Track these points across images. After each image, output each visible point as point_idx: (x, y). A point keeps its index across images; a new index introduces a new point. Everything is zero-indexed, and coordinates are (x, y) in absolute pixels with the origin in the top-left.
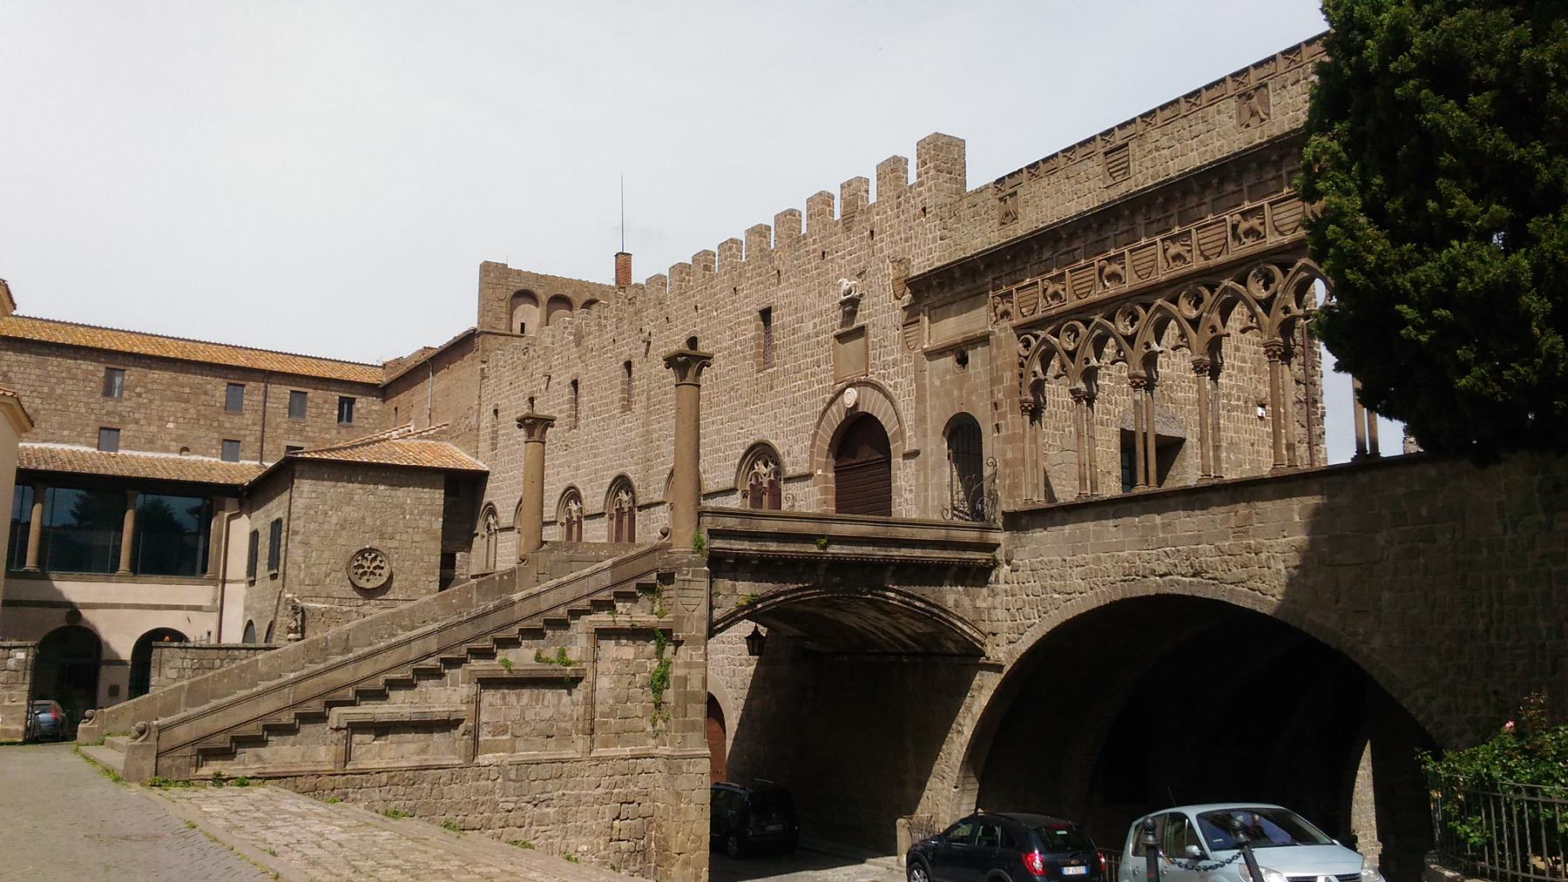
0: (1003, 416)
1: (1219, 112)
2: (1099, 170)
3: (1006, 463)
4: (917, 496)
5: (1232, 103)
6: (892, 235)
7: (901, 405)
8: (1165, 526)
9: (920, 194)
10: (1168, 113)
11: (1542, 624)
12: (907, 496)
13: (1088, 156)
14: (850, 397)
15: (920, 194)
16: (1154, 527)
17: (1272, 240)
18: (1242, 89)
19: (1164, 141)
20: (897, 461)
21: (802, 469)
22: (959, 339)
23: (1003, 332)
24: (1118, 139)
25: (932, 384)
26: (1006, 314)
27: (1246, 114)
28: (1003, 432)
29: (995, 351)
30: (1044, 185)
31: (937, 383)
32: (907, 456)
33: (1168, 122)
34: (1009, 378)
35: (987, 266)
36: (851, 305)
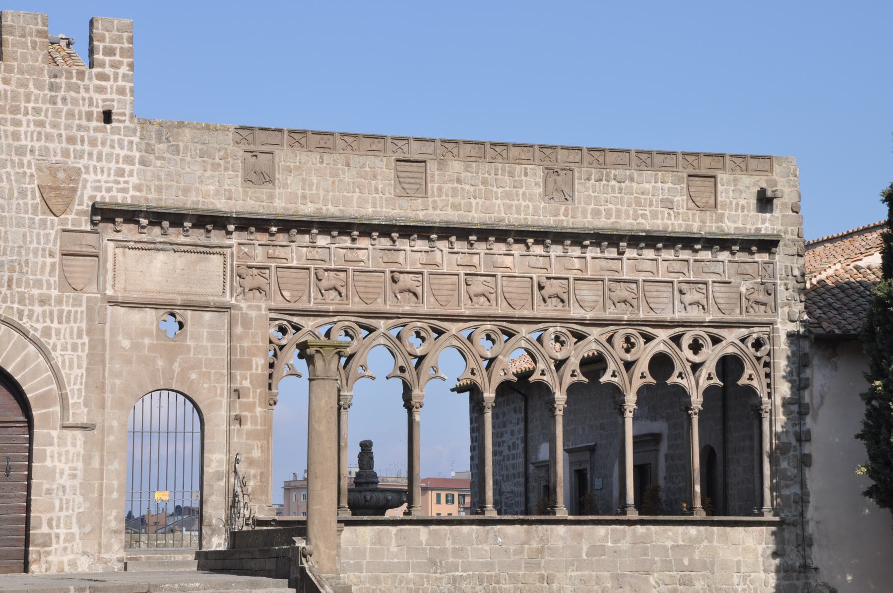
0: (251, 407)
5: (540, 171)
6: (41, 124)
8: (456, 552)
12: (64, 481)
15: (100, 90)
16: (443, 551)
17: (575, 312)
22: (179, 299)
23: (255, 310)
24: (415, 151)
27: (551, 186)
28: (248, 426)
29: (239, 330)
31: (126, 343)
34: (259, 363)
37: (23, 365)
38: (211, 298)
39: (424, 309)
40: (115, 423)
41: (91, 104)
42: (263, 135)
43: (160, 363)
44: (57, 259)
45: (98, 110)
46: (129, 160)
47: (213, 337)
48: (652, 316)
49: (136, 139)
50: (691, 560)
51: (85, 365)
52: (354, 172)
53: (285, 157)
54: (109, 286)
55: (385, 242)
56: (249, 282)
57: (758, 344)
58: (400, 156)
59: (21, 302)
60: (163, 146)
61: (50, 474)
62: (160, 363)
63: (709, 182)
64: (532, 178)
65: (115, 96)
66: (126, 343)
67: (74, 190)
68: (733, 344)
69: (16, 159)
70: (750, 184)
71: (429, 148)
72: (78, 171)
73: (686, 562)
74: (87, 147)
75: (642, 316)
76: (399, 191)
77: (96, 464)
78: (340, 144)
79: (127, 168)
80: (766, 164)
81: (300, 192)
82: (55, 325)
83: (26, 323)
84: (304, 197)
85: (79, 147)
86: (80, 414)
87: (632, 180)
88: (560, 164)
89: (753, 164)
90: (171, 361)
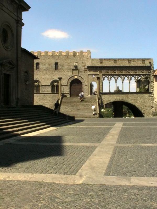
5: (128, 61)
13: (112, 60)
14: (76, 77)
20: (83, 85)
21: (66, 84)
24: (115, 60)
26: (101, 73)
30: (106, 61)
32: (85, 85)
33: (121, 60)
39: (116, 74)
45: (87, 58)
55: (113, 68)
57: (149, 76)
63: (144, 61)
64: (127, 62)
75: (138, 74)
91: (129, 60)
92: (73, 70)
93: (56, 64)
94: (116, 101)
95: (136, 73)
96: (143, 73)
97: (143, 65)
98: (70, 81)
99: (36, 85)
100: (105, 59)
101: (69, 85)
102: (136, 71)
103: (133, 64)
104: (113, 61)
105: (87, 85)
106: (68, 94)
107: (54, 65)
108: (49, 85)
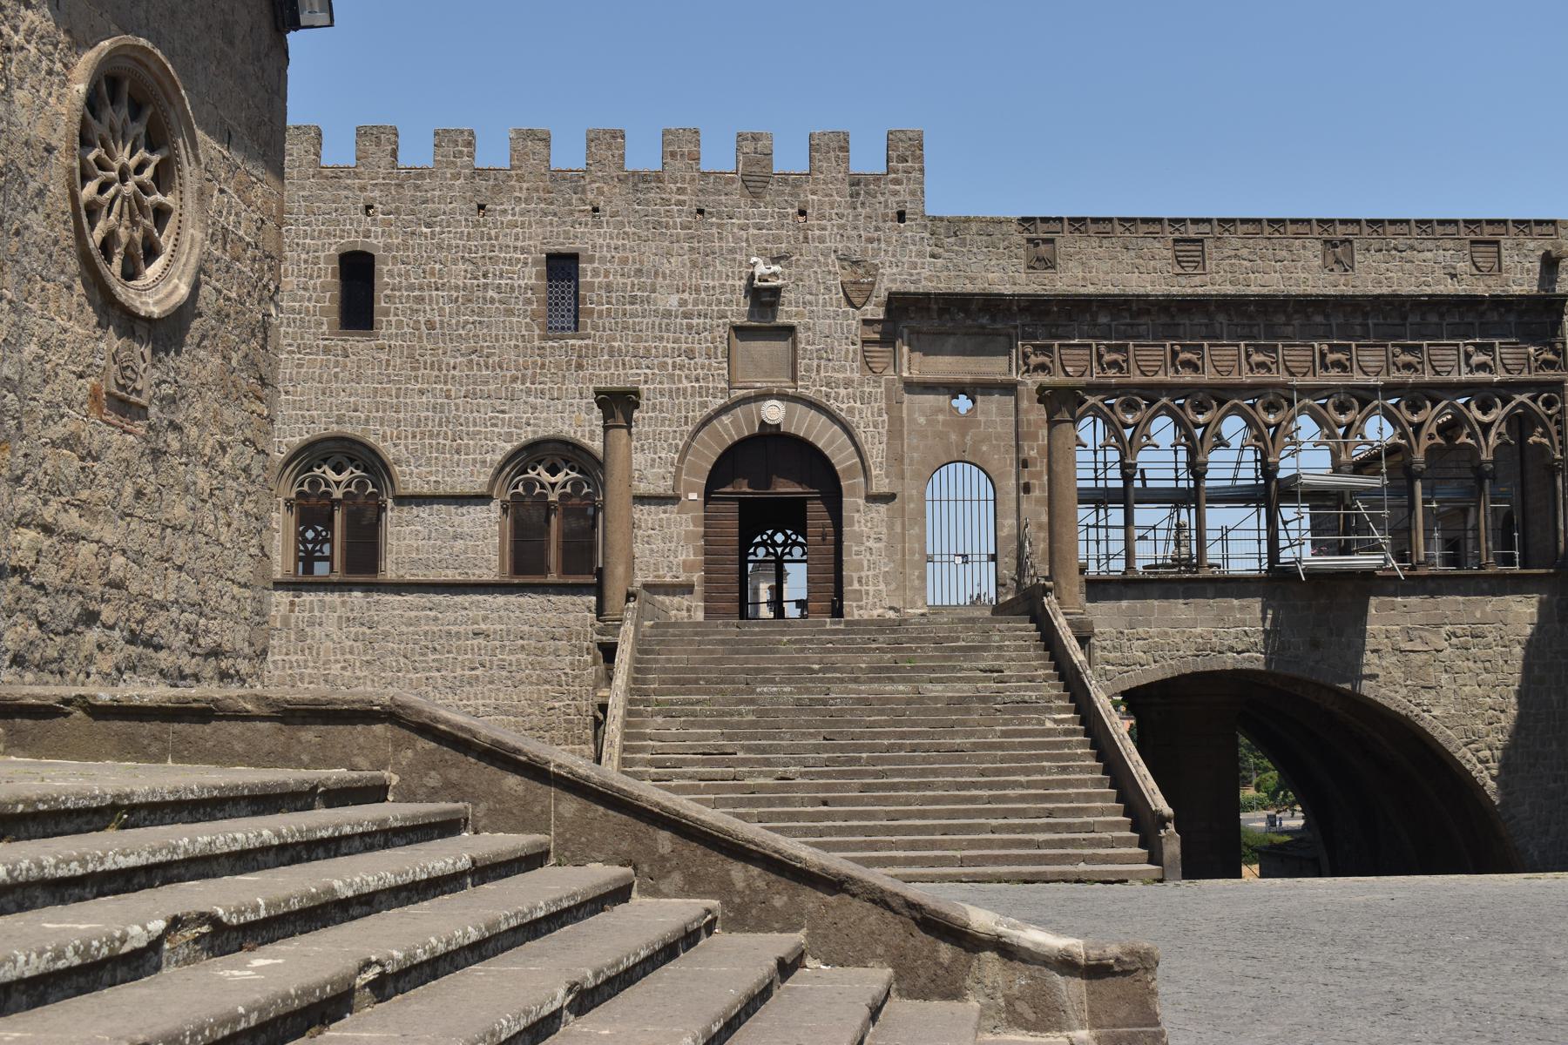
1: (1304, 247)
2: (1169, 254)
3: (1040, 526)
4: (890, 546)
5: (1319, 245)
6: (842, 227)
7: (861, 435)
9: (895, 193)
10: (1250, 228)
11: (1554, 697)
12: (871, 544)
13: (1154, 236)
14: (773, 412)
17: (1358, 378)
18: (1325, 236)
19: (1244, 252)
20: (852, 502)
21: (663, 487)
24: (1192, 232)
25: (912, 420)
27: (1330, 259)
30: (1088, 245)
31: (922, 420)
32: (873, 498)
35: (1021, 310)
36: (764, 298)
37: (831, 442)
38: (998, 377)
40: (914, 492)
41: (886, 206)
42: (1045, 226)
43: (953, 437)
44: (859, 346)
45: (892, 212)
46: (920, 254)
47: (1001, 412)
48: (1438, 378)
49: (926, 235)
50: (1483, 612)
51: (885, 439)
52: (1132, 253)
53: (1066, 242)
54: (905, 368)
55: (1164, 319)
56: (1033, 360)
58: (1177, 235)
59: (828, 385)
60: (952, 240)
61: (859, 539)
62: (953, 437)
64: (1311, 252)
65: (908, 198)
66: (922, 420)
67: (873, 284)
68: (1522, 404)
69: (821, 258)
70: (1536, 246)
71: (1206, 228)
72: (876, 267)
73: (1478, 615)
74: (883, 246)
75: (1427, 378)
76: (1178, 270)
77: (898, 529)
78: (1119, 229)
79: (919, 261)
80: (1551, 229)
81: (1080, 275)
82: (858, 404)
83: (833, 405)
84: (1084, 279)
85: (875, 245)
86: (881, 485)
87: (1412, 248)
88: (1337, 237)
89: (1537, 230)
90: (963, 436)
91: (1340, 232)
92: (740, 332)
93: (562, 267)
94: (1201, 665)
95: (1408, 366)
96: (1482, 367)
97: (1481, 289)
98: (708, 454)
99: (338, 494)
100: (1078, 223)
101: (693, 496)
102: (1406, 349)
103: (1377, 274)
104: (1162, 250)
105: (888, 498)
106: (688, 589)
107: (531, 276)
108: (484, 490)
